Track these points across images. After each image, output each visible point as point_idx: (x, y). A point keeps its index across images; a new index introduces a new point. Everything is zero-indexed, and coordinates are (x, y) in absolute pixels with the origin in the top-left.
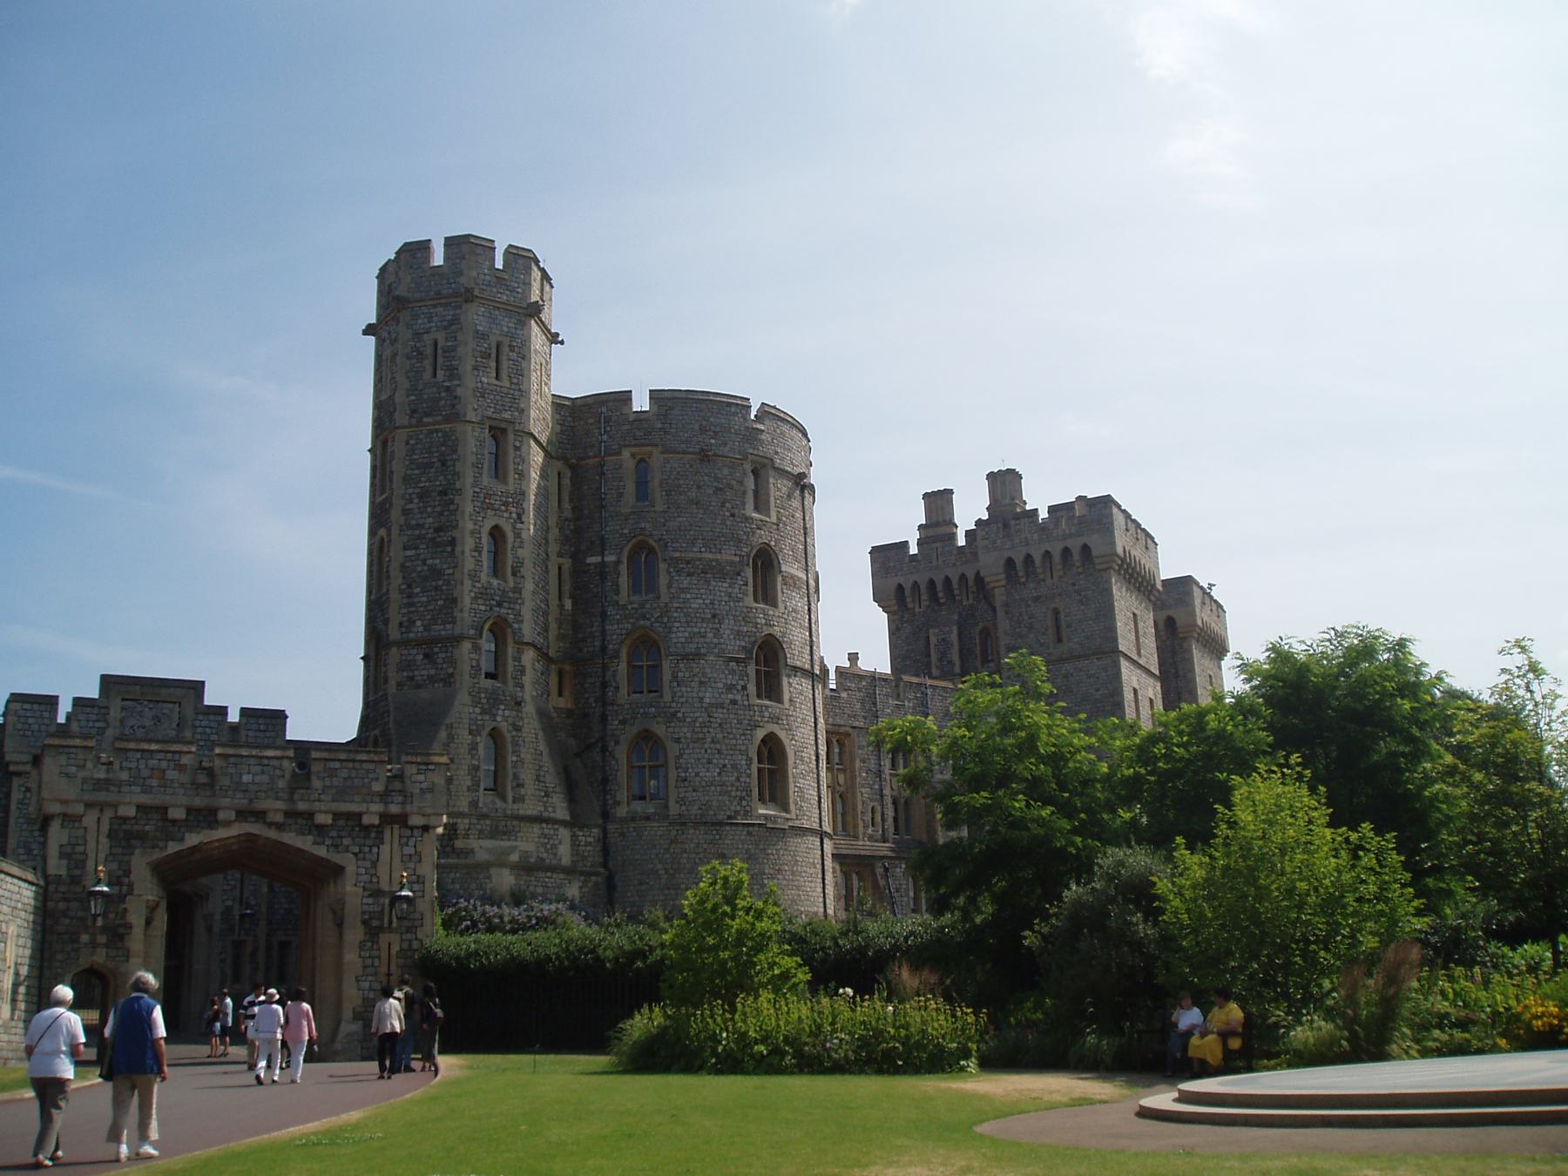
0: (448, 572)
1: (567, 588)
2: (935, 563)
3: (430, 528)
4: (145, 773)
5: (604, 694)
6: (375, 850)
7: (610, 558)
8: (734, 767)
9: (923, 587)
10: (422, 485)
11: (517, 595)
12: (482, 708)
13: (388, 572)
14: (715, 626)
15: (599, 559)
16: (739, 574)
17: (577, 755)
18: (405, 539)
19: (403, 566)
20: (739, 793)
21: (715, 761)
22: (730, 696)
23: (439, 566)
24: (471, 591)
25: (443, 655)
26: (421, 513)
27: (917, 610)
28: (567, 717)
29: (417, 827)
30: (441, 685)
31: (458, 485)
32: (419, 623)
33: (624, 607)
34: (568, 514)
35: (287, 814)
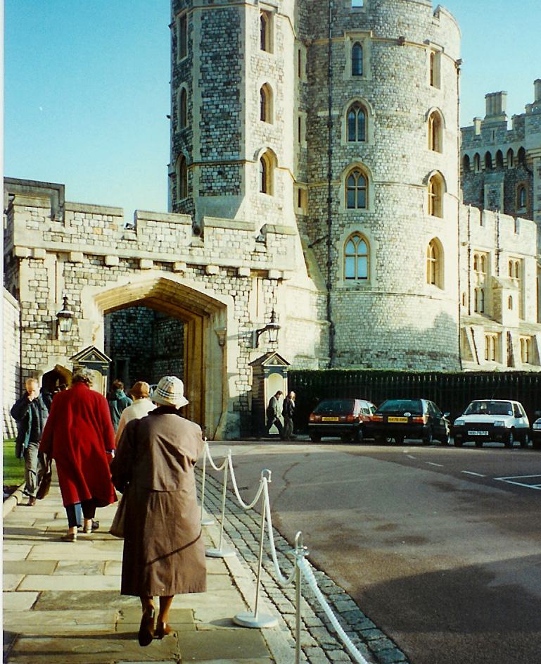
0: (234, 114)
1: (304, 132)
2: (492, 141)
3: (220, 82)
4: (89, 230)
5: (330, 207)
6: (246, 293)
7: (335, 113)
8: (413, 258)
9: (482, 157)
10: (214, 50)
11: (279, 134)
12: (258, 211)
13: (190, 113)
14: (405, 163)
15: (327, 113)
16: (420, 128)
17: (310, 246)
18: (203, 90)
19: (202, 109)
20: (416, 276)
21: (402, 254)
22: (413, 212)
23: (227, 110)
24: (251, 129)
25: (232, 173)
26: (214, 71)
27: (476, 172)
28: (304, 221)
29: (275, 279)
30: (231, 193)
31: (240, 52)
32: (214, 150)
33: (344, 148)
34: (305, 80)
35: (189, 265)
